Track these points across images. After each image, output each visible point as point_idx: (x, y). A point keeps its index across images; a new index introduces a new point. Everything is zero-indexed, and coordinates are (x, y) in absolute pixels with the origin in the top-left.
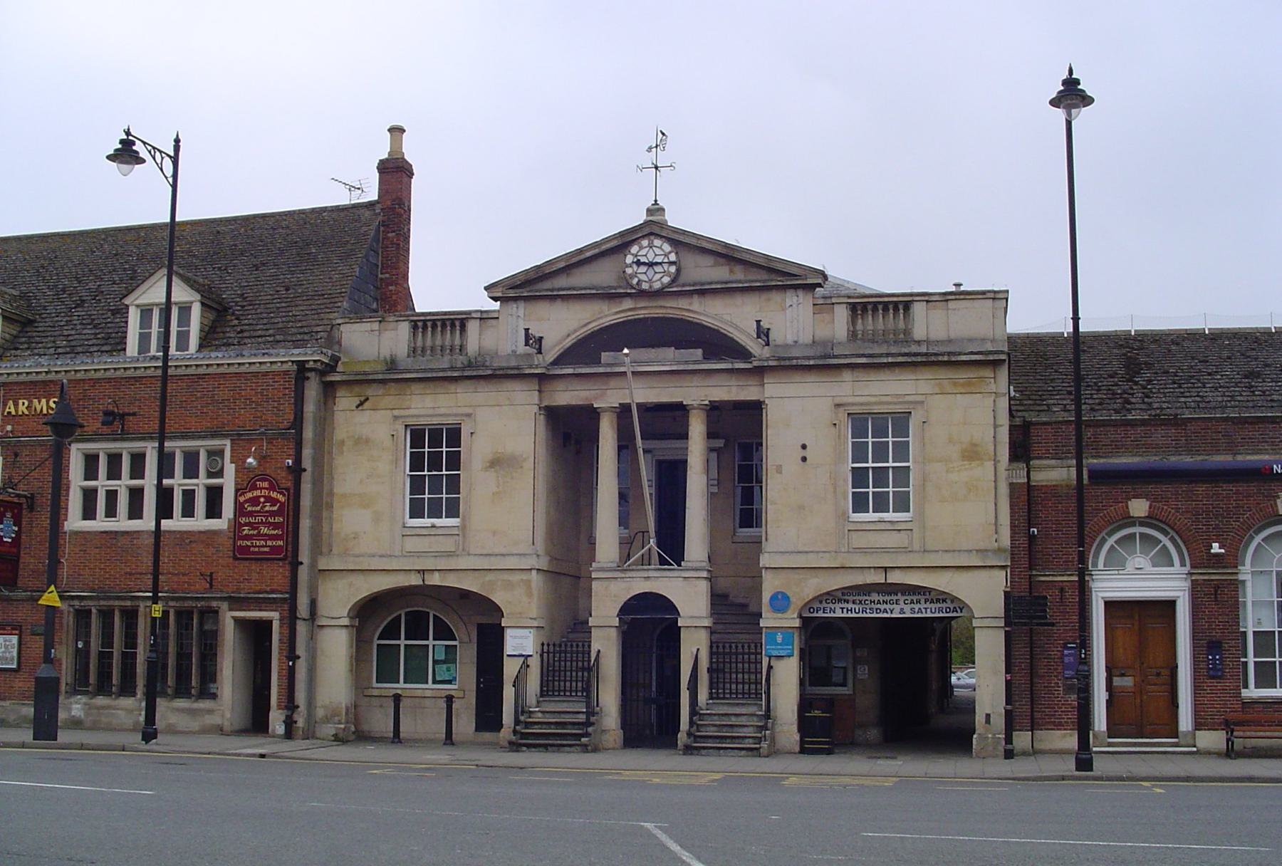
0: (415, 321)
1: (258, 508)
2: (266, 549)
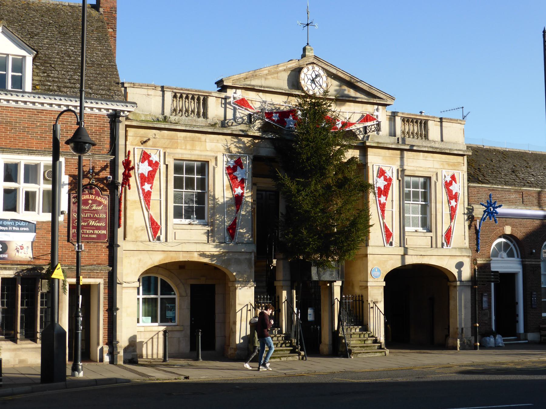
0: (175, 93)
1: (87, 208)
2: (95, 236)
